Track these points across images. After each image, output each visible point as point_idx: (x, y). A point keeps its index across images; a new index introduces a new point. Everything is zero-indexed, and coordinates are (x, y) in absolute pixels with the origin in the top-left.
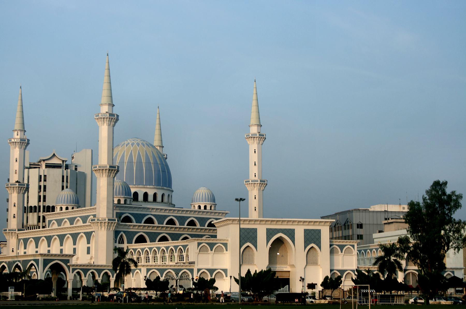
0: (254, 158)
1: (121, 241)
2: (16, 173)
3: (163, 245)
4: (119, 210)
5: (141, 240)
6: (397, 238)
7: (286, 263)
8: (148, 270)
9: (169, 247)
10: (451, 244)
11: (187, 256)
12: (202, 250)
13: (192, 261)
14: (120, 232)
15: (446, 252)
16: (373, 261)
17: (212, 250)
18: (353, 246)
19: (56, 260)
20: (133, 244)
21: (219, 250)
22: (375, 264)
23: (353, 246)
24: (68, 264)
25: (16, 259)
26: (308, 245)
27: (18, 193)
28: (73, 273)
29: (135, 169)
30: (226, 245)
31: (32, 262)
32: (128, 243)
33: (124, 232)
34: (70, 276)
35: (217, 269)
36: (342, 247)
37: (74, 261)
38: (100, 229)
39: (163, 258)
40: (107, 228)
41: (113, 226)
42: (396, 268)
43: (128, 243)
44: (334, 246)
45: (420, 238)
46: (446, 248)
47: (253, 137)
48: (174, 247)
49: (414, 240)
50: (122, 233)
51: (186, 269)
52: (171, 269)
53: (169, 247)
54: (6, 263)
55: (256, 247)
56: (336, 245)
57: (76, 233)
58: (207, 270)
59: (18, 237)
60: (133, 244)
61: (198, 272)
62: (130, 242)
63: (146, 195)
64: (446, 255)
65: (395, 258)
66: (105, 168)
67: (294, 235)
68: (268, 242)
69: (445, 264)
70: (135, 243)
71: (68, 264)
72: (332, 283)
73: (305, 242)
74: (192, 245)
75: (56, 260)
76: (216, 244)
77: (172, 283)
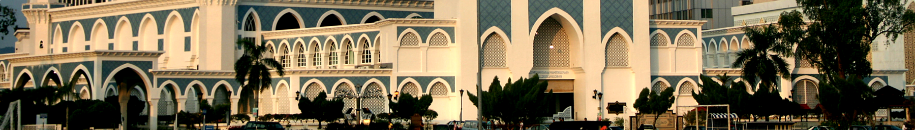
1: (251, 26)
3: (330, 32)
5: (288, 22)
6: (778, 14)
7: (566, 65)
8: (303, 81)
9: (342, 36)
10: (882, 24)
11: (378, 52)
12: (405, 41)
13: (387, 61)
14: (248, 7)
15: (872, 39)
16: (733, 59)
17: (424, 41)
18: (694, 31)
19: (126, 62)
20: (274, 31)
21: (439, 41)
22: (736, 65)
23: (694, 31)
24: (150, 70)
25: (49, 62)
26: (609, 30)
30: (451, 31)
31: (81, 67)
32: (263, 29)
33: (256, 8)
34: (154, 94)
35: (683, 77)
36: (672, 33)
37: (160, 64)
39: (331, 57)
42: (776, 72)
43: (263, 29)
44: (658, 31)
45: (821, 15)
46: (871, 33)
48: (353, 35)
49: (810, 18)
50: (252, 10)
51: (376, 77)
52: (346, 78)
53: (342, 36)
54: (29, 68)
55: (509, 34)
56: (662, 29)
57: (163, 11)
58: (416, 78)
59: (50, 20)
60: (274, 31)
61: (398, 84)
62: (266, 27)
64: (871, 46)
65: (775, 54)
67: (582, 11)
68: (531, 25)
69: (869, 64)
70: (277, 29)
71: (150, 70)
72: (654, 101)
73: (602, 24)
74: (387, 32)
75: (126, 62)
76: (432, 29)
77: (350, 104)
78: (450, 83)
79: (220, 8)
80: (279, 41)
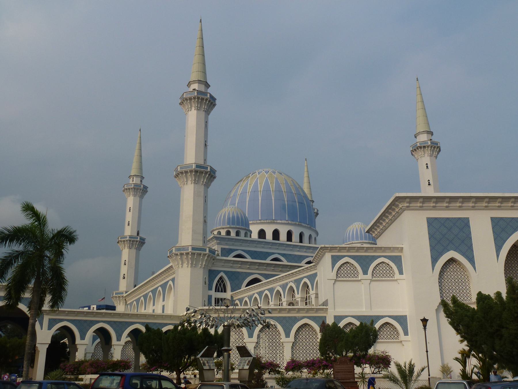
0: (426, 175)
2: (129, 225)
4: (227, 244)
9: (287, 284)
14: (219, 272)
17: (365, 273)
21: (383, 273)
27: (130, 248)
28: (50, 328)
29: (260, 199)
30: (398, 261)
33: (226, 273)
38: (180, 266)
40: (192, 264)
41: (203, 260)
47: (423, 147)
59: (126, 302)
63: (276, 234)
66: (188, 169)
76: (375, 258)
78: (401, 324)
79: (189, 269)
80: (243, 298)
